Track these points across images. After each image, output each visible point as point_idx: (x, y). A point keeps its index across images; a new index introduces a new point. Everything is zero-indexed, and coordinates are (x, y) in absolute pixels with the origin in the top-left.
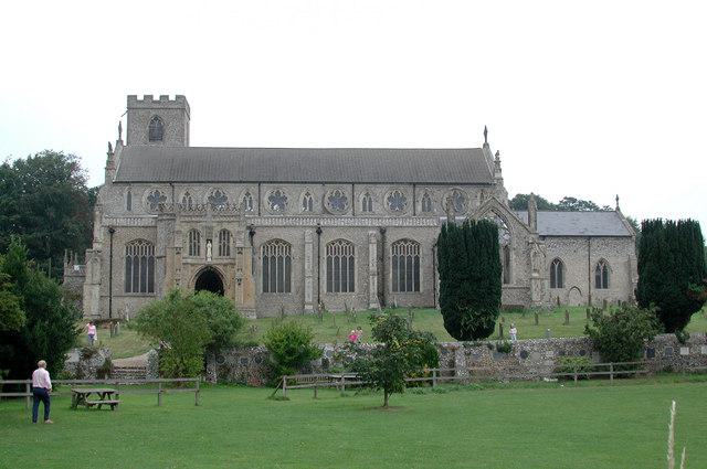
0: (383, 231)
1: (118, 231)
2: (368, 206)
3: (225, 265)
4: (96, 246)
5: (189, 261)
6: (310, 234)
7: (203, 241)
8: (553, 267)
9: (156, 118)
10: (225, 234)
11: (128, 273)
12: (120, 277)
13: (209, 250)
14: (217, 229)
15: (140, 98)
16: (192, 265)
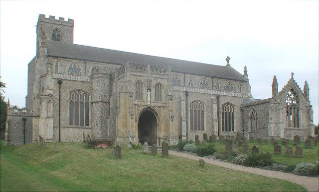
0: (218, 97)
1: (64, 82)
3: (160, 107)
5: (136, 102)
6: (182, 95)
7: (144, 89)
10: (159, 86)
11: (71, 112)
12: (66, 114)
14: (154, 82)
16: (138, 105)
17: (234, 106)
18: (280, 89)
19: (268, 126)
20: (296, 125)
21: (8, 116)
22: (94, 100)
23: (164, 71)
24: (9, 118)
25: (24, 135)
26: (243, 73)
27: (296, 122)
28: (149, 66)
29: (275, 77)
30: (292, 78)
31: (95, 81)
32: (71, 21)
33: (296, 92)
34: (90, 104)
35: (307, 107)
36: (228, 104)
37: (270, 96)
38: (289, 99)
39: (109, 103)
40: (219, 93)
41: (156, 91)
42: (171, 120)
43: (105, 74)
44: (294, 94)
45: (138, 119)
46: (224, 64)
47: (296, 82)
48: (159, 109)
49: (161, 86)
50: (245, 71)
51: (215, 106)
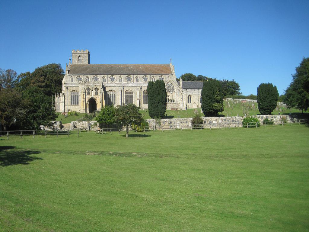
1: (68, 88)
2: (137, 80)
4: (63, 92)
8: (188, 97)
12: (69, 100)
14: (95, 87)
41: (95, 91)
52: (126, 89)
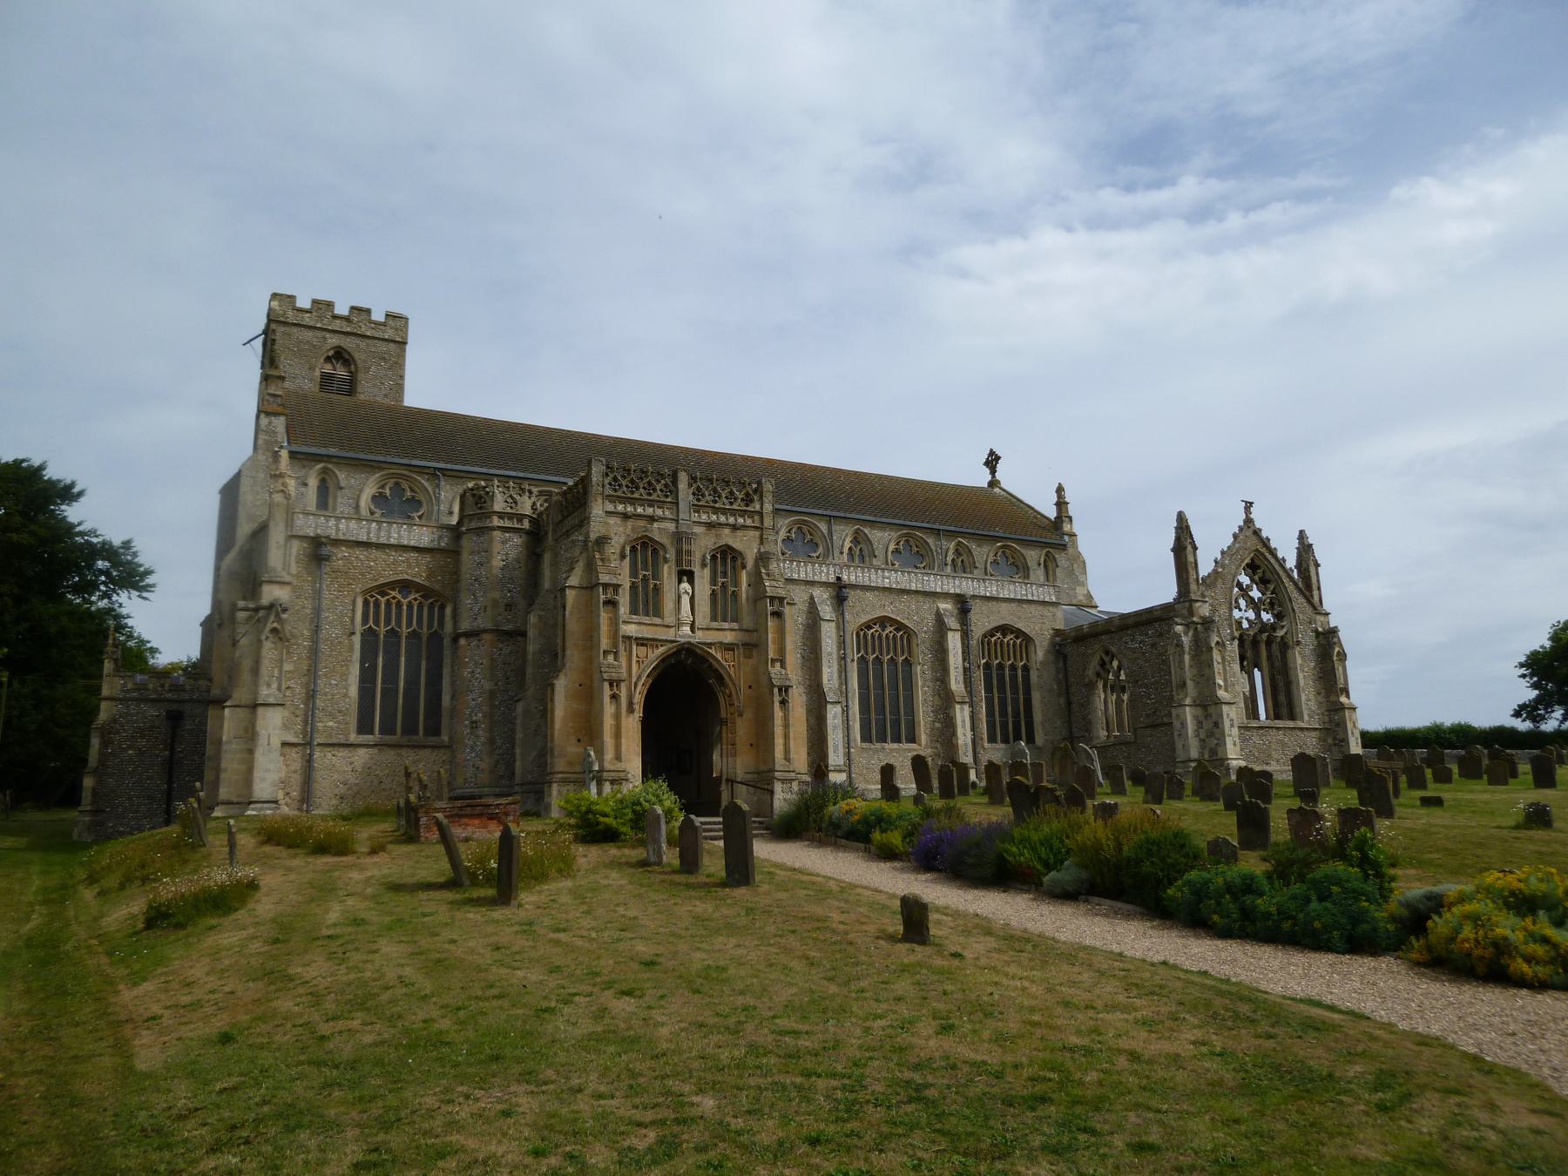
3: (729, 647)
7: (668, 572)
9: (340, 355)
11: (367, 677)
13: (685, 600)
14: (703, 544)
15: (304, 302)
16: (642, 642)
17: (1028, 640)
18: (1205, 567)
19: (1170, 715)
20: (1284, 711)
21: (103, 705)
22: (465, 625)
23: (748, 500)
24: (105, 712)
25: (170, 782)
26: (1051, 513)
27: (1282, 698)
28: (683, 478)
29: (1181, 519)
30: (1249, 521)
31: (467, 543)
32: (397, 321)
33: (1268, 575)
34: (447, 642)
35: (1316, 631)
36: (1004, 629)
37: (1166, 592)
38: (1242, 603)
39: (524, 634)
40: (966, 586)
41: (713, 581)
42: (777, 699)
43: (511, 516)
44: (1263, 583)
45: (639, 699)
46: (979, 478)
47: (1264, 534)
48: (729, 655)
49: (734, 559)
50: (1061, 504)
51: (954, 641)
52: (862, 609)
